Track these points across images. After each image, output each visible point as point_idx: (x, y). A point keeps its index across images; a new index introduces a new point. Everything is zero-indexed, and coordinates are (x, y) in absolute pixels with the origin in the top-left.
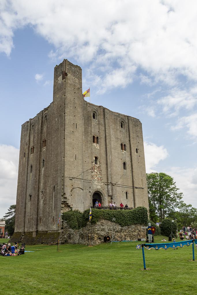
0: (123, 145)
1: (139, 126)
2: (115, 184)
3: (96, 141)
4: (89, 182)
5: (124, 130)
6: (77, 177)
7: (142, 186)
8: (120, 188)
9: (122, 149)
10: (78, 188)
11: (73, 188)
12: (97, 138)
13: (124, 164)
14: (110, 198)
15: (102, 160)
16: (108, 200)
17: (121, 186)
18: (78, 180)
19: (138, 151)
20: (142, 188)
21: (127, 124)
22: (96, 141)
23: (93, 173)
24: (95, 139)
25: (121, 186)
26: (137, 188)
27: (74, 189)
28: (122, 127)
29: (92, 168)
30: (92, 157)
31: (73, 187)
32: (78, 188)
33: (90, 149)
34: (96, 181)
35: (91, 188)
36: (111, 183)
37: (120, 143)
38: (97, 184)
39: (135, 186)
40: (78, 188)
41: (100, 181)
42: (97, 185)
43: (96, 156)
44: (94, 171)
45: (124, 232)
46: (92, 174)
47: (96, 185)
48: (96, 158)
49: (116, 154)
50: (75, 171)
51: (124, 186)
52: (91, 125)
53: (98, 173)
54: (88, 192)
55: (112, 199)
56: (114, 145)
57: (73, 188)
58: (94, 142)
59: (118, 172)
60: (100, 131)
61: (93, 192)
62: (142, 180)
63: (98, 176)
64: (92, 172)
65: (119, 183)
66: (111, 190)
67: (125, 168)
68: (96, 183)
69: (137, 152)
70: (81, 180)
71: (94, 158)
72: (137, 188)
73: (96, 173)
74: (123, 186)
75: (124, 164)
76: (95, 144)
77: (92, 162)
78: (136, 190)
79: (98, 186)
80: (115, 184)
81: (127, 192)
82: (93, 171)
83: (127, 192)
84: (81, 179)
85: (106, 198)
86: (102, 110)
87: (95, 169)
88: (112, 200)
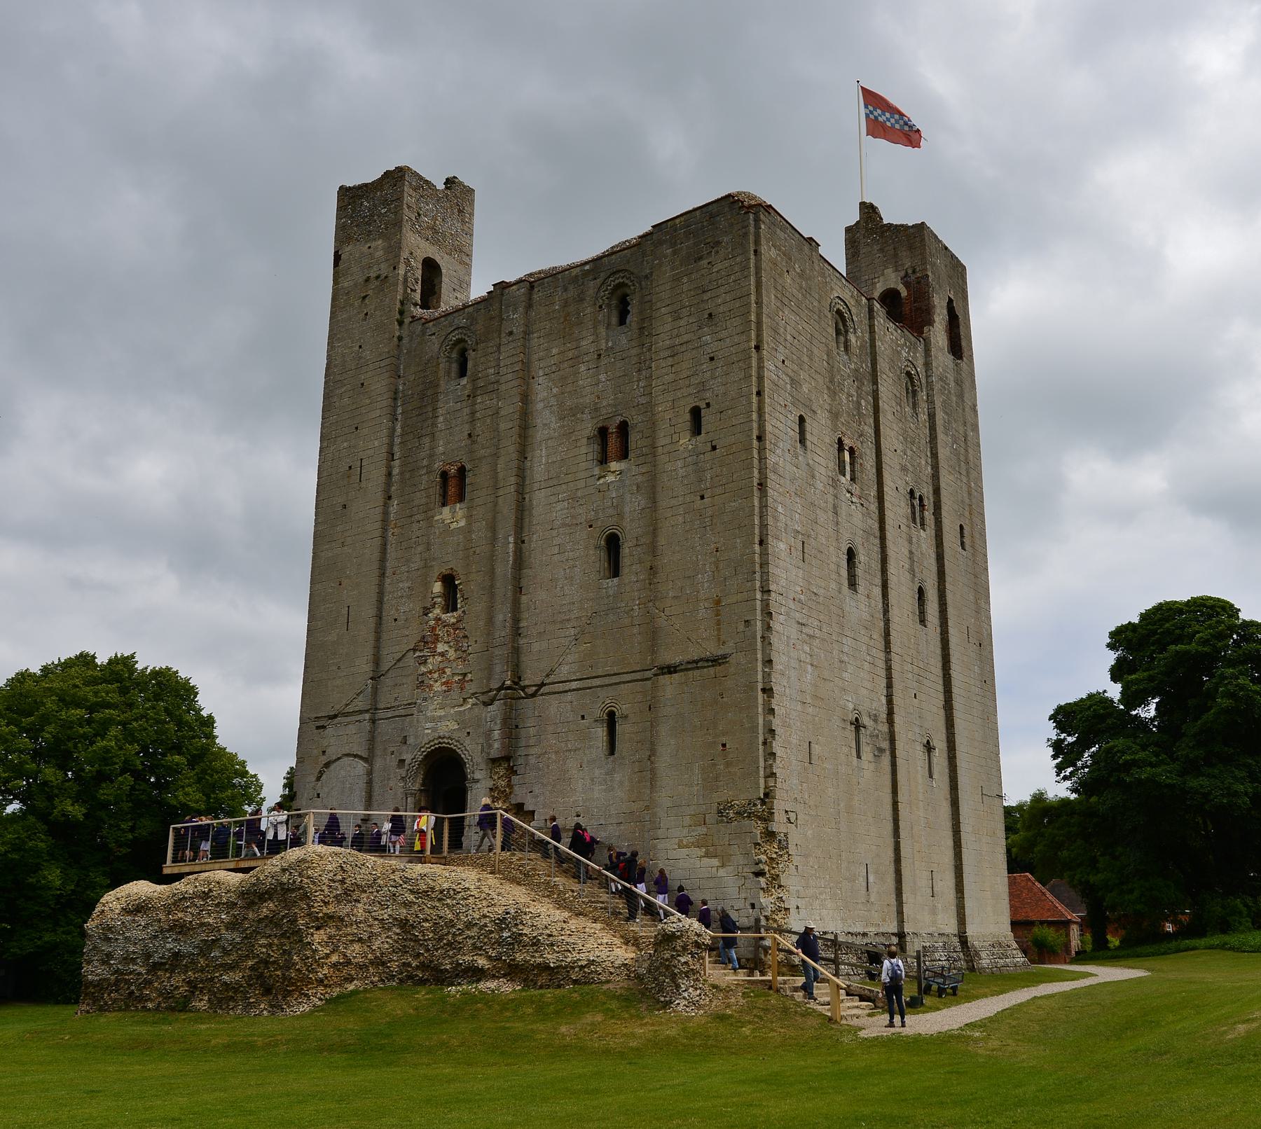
0: (612, 429)
2: (543, 685)
3: (452, 490)
4: (403, 712)
5: (623, 339)
6: (350, 709)
7: (712, 649)
8: (569, 696)
10: (348, 755)
11: (327, 765)
12: (462, 471)
13: (613, 544)
16: (490, 784)
18: (348, 719)
19: (707, 418)
20: (716, 661)
22: (452, 490)
23: (425, 662)
24: (454, 485)
25: (574, 685)
26: (670, 670)
27: (332, 767)
29: (424, 637)
30: (427, 585)
31: (323, 760)
32: (346, 759)
33: (419, 549)
35: (411, 741)
37: (588, 427)
40: (348, 755)
41: (455, 694)
44: (434, 653)
47: (433, 720)
48: (449, 581)
49: (559, 506)
50: (338, 682)
52: (434, 425)
53: (452, 654)
57: (327, 765)
62: (718, 602)
63: (448, 671)
65: (564, 671)
66: (498, 727)
69: (697, 428)
70: (358, 718)
71: (438, 587)
72: (670, 670)
73: (440, 659)
75: (613, 544)
77: (426, 611)
79: (441, 719)
81: (611, 715)
83: (611, 715)
84: (361, 712)
87: (436, 639)
88: (515, 779)
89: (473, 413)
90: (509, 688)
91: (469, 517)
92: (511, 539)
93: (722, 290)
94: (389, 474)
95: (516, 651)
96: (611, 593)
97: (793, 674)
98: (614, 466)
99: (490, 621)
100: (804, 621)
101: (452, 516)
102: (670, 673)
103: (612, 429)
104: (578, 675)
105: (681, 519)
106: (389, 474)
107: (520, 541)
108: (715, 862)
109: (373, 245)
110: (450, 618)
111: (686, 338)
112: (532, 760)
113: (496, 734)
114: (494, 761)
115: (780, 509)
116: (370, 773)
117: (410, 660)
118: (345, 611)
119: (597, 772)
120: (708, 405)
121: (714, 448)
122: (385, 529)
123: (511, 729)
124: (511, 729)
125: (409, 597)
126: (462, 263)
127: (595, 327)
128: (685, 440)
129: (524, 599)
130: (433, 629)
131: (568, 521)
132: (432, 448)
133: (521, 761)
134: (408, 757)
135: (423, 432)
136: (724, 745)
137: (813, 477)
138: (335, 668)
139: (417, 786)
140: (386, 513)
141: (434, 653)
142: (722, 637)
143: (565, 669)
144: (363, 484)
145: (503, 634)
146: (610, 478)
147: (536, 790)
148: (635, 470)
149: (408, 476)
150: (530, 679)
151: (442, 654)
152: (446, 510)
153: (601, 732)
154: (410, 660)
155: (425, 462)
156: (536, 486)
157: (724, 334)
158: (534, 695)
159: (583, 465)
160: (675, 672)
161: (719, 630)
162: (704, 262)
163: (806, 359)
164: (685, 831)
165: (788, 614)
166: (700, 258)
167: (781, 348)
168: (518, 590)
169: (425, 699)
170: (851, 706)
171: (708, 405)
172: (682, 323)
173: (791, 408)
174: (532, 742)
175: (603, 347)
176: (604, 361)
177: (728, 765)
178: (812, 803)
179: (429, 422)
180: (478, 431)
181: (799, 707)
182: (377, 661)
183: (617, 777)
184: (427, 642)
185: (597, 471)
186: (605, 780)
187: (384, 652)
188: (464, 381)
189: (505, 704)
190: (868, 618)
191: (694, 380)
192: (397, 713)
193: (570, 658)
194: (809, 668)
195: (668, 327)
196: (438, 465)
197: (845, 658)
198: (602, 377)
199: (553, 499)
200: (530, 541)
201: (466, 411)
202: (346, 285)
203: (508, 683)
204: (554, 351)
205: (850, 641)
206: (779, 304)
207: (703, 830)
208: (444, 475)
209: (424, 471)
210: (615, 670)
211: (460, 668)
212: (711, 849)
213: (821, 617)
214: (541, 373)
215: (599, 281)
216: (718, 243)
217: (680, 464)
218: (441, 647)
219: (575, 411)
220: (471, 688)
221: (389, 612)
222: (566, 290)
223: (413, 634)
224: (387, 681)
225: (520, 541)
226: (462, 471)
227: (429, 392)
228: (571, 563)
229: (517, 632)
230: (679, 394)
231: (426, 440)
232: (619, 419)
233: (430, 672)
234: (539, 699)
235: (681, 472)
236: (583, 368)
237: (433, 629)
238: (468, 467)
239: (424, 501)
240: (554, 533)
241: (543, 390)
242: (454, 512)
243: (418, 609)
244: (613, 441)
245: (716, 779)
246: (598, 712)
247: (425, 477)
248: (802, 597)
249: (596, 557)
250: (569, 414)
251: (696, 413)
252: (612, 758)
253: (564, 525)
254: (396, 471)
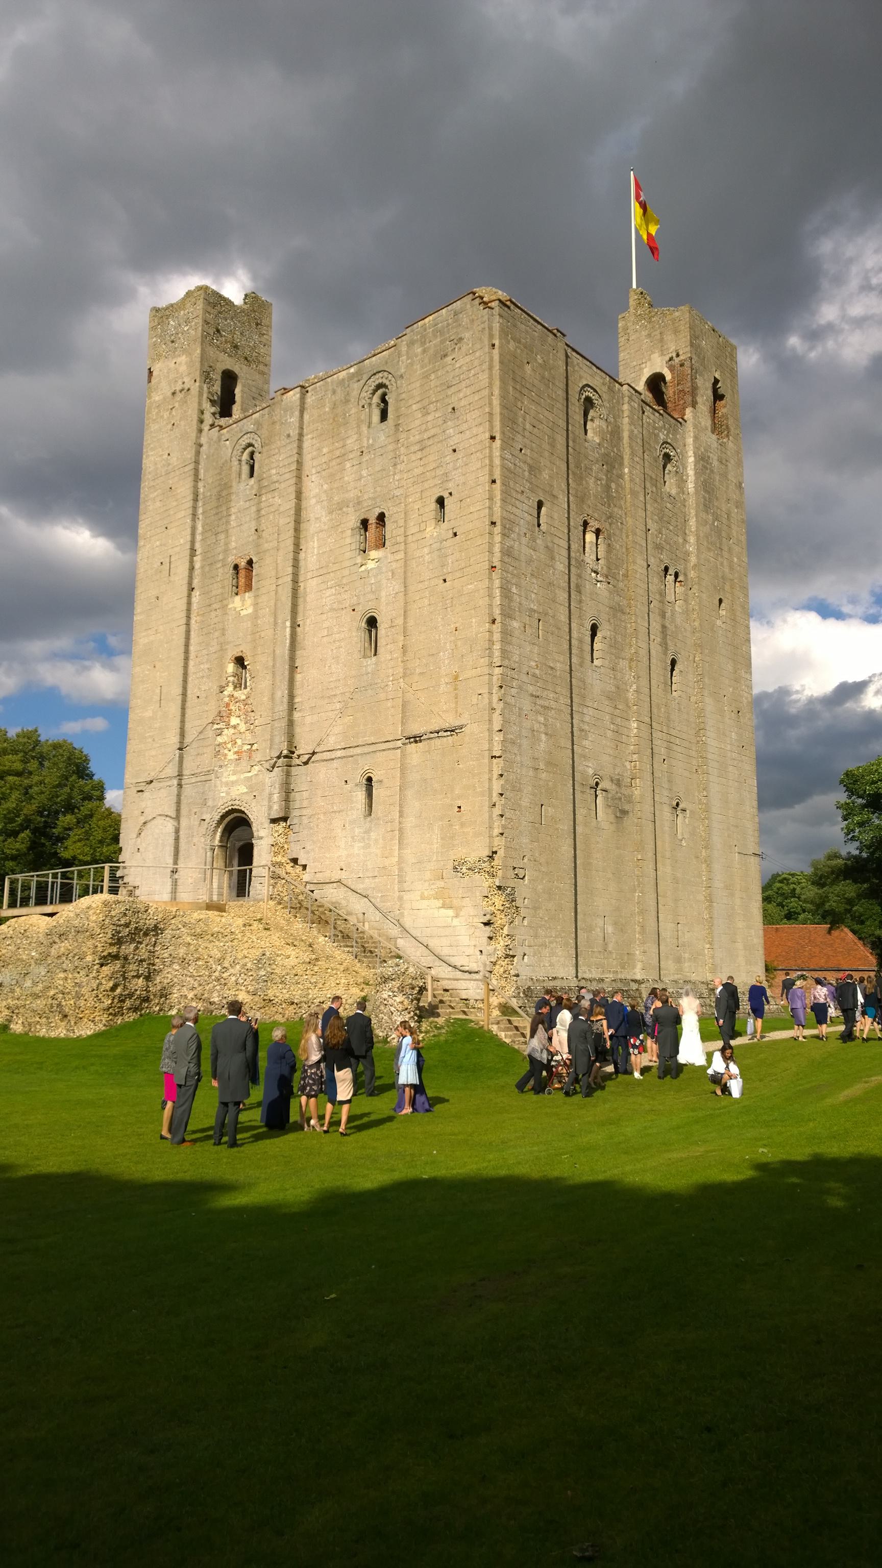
1: (467, 335)
2: (314, 753)
4: (204, 778)
5: (382, 434)
7: (451, 721)
8: (335, 764)
12: (250, 562)
16: (271, 841)
17: (339, 754)
18: (161, 785)
22: (242, 581)
24: (244, 574)
25: (339, 754)
26: (417, 739)
27: (148, 825)
29: (220, 712)
30: (222, 667)
31: (142, 819)
33: (217, 634)
34: (231, 767)
35: (210, 803)
37: (353, 521)
38: (233, 778)
42: (233, 783)
44: (228, 726)
46: (220, 739)
47: (227, 784)
48: (240, 661)
49: (329, 592)
50: (153, 753)
51: (358, 751)
52: (228, 522)
53: (243, 727)
59: (332, 685)
63: (239, 742)
65: (331, 742)
66: (277, 791)
68: (228, 775)
71: (231, 668)
72: (417, 739)
75: (372, 622)
80: (314, 753)
82: (222, 725)
83: (370, 780)
84: (171, 778)
85: (262, 833)
88: (292, 836)
89: (259, 511)
90: (286, 757)
91: (256, 605)
92: (288, 624)
93: (463, 384)
94: (192, 569)
95: (291, 723)
96: (369, 670)
97: (525, 743)
98: (374, 554)
99: (272, 698)
100: (538, 694)
101: (242, 604)
102: (416, 742)
103: (372, 520)
104: (343, 745)
105: (426, 602)
106: (192, 569)
107: (295, 626)
108: (451, 912)
109: (178, 360)
110: (241, 694)
111: (432, 432)
112: (305, 820)
113: (276, 797)
114: (274, 821)
115: (514, 590)
116: (177, 831)
117: (210, 733)
118: (158, 691)
119: (357, 831)
120: (451, 494)
121: (455, 534)
122: (188, 617)
123: (287, 793)
124: (287, 793)
125: (208, 677)
126: (263, 373)
127: (358, 426)
128: (431, 530)
129: (298, 677)
130: (228, 705)
131: (335, 606)
132: (226, 544)
133: (295, 821)
134: (207, 817)
135: (220, 529)
136: (460, 807)
137: (553, 558)
138: (150, 740)
139: (217, 842)
140: (189, 603)
141: (228, 726)
142: (459, 710)
143: (332, 739)
144: (172, 578)
145: (281, 708)
146: (371, 565)
147: (308, 848)
148: (391, 557)
149: (207, 569)
150: (303, 749)
151: (235, 727)
152: (237, 598)
153: (361, 795)
154: (210, 733)
155: (221, 557)
156: (309, 575)
157: (464, 427)
158: (306, 763)
159: (348, 555)
160: (421, 741)
161: (457, 703)
162: (449, 359)
163: (546, 446)
164: (427, 884)
165: (520, 688)
166: (445, 356)
167: (519, 438)
168: (293, 669)
169: (221, 767)
170: (591, 771)
171: (451, 494)
172: (430, 418)
173: (529, 493)
174: (305, 804)
175: (365, 445)
176: (366, 458)
177: (462, 825)
178: (542, 860)
179: (224, 520)
180: (263, 527)
181: (531, 773)
182: (182, 734)
183: (373, 835)
184: (222, 716)
185: (359, 560)
186: (363, 838)
187: (188, 726)
188: (252, 481)
189: (282, 771)
190: (613, 689)
191: (440, 472)
192: (199, 779)
193: (337, 730)
194: (543, 737)
195: (418, 422)
196: (231, 559)
197: (586, 727)
198: (364, 473)
199: (323, 586)
200: (304, 624)
201: (254, 509)
202: (157, 398)
203: (285, 752)
204: (325, 450)
205: (591, 712)
206: (517, 395)
207: (441, 884)
208: (236, 567)
209: (219, 565)
210: (373, 740)
211: (249, 737)
212: (448, 901)
213: (558, 689)
214: (314, 471)
215: (362, 382)
216: (461, 339)
217: (426, 550)
218: (234, 721)
219: (341, 506)
220: (257, 757)
221: (191, 692)
222: (334, 392)
223: (212, 709)
224: (189, 753)
225: (295, 626)
226: (250, 562)
227: (224, 493)
228: (338, 644)
229: (291, 707)
230: (426, 485)
231: (222, 536)
232: (377, 512)
233: (225, 743)
234: (310, 765)
235: (427, 558)
236: (348, 465)
237: (228, 705)
238: (254, 560)
239: (220, 591)
240: (324, 617)
241: (313, 487)
242: (243, 601)
243: (215, 688)
245: (452, 838)
247: (220, 570)
248: (537, 672)
250: (337, 508)
251: (441, 502)
252: (369, 819)
253: (332, 609)
254: (197, 565)
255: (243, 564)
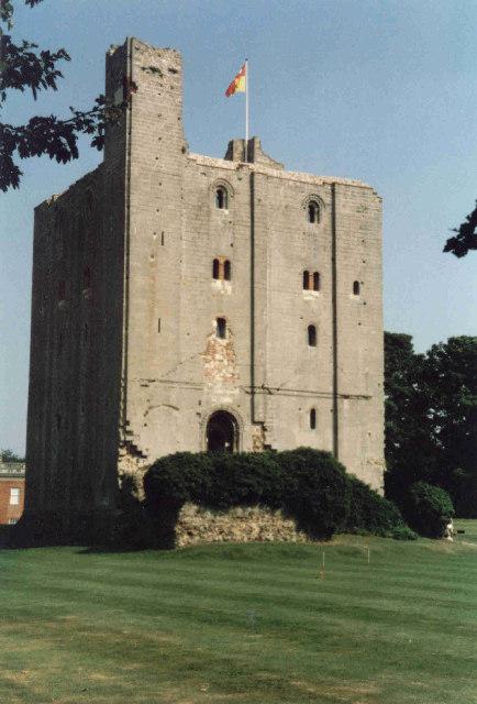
3: (221, 271)
7: (364, 393)
8: (294, 399)
9: (306, 286)
11: (151, 408)
12: (227, 264)
13: (312, 331)
14: (259, 427)
15: (239, 324)
19: (362, 288)
20: (366, 398)
21: (329, 209)
22: (221, 271)
24: (221, 269)
26: (346, 397)
28: (312, 220)
36: (263, 387)
37: (301, 270)
39: (341, 391)
43: (220, 315)
45: (258, 519)
46: (207, 365)
48: (222, 322)
53: (226, 362)
54: (194, 414)
55: (264, 429)
56: (280, 277)
58: (216, 276)
60: (237, 244)
61: (208, 411)
64: (207, 361)
67: (312, 339)
71: (215, 324)
72: (346, 397)
74: (301, 393)
75: (312, 331)
76: (218, 284)
78: (345, 405)
79: (225, 396)
82: (210, 357)
86: (246, 180)
87: (215, 352)
88: (266, 433)
177: (372, 442)
184: (210, 350)
218: (218, 356)
238: (231, 260)
244: (310, 280)
246: (308, 408)
249: (305, 335)
255: (222, 261)
